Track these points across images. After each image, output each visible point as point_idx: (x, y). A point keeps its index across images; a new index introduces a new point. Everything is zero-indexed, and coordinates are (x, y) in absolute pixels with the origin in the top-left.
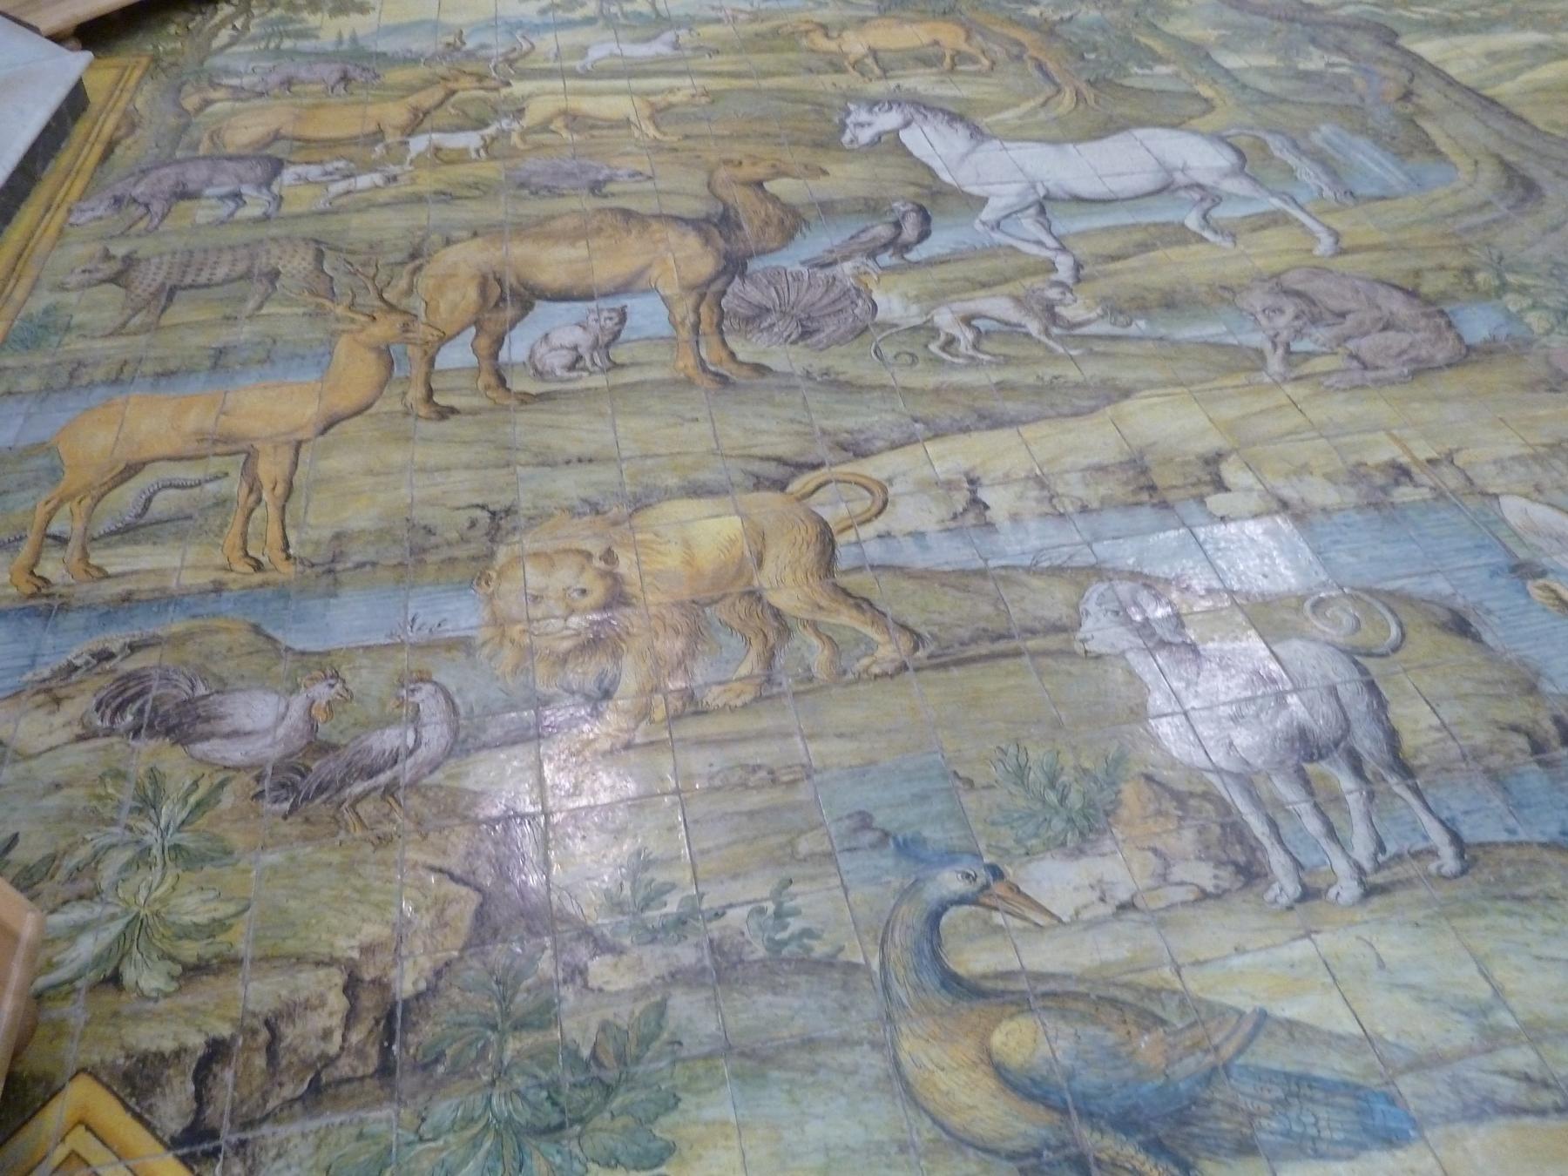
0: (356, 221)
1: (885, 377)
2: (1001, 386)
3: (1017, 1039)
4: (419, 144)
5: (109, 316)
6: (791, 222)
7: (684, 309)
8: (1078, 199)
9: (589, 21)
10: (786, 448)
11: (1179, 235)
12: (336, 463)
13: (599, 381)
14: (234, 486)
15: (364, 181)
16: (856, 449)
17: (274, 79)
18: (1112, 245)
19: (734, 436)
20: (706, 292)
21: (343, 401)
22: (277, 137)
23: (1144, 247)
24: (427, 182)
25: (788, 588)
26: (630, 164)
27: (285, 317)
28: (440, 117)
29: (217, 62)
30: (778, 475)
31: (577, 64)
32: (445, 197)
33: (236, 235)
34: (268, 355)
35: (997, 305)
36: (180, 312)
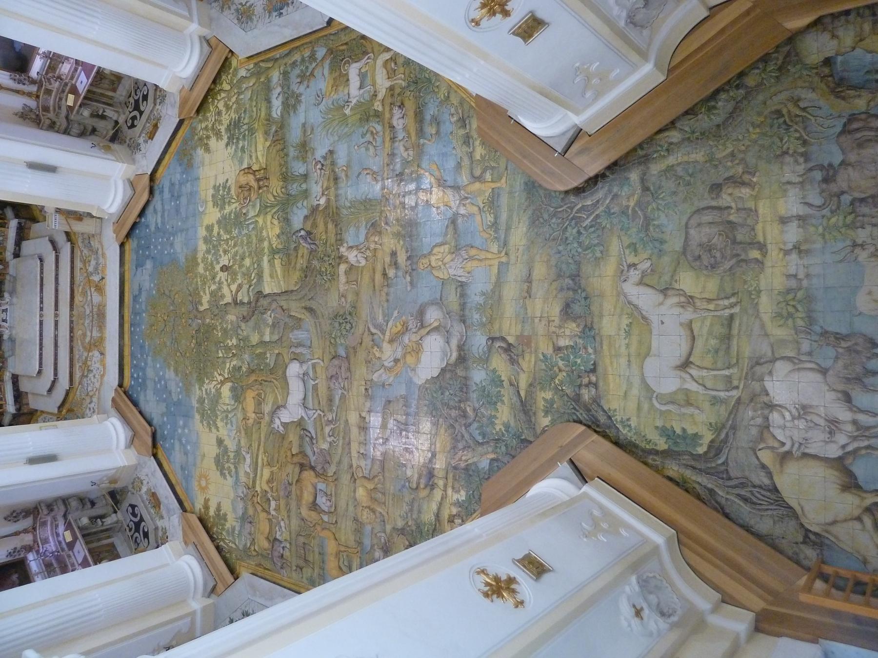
0: (293, 528)
1: (339, 456)
2: (344, 438)
3: (422, 486)
4: (273, 513)
5: (310, 571)
6: (302, 453)
7: (321, 480)
8: (304, 399)
9: (236, 468)
10: (349, 476)
11: (315, 388)
12: (343, 539)
13: (333, 499)
14: (345, 554)
15: (282, 524)
16: (351, 466)
17: (249, 536)
18: (316, 402)
19: (346, 482)
20: (318, 475)
21: (333, 537)
22: (267, 538)
23: (317, 395)
24: (284, 513)
25: (371, 486)
26: (284, 476)
27: (314, 543)
28: (266, 507)
29: (241, 547)
30: (354, 479)
31: (252, 476)
32: (289, 511)
33: (293, 549)
34: (322, 546)
35: (327, 430)
36: (311, 559)
